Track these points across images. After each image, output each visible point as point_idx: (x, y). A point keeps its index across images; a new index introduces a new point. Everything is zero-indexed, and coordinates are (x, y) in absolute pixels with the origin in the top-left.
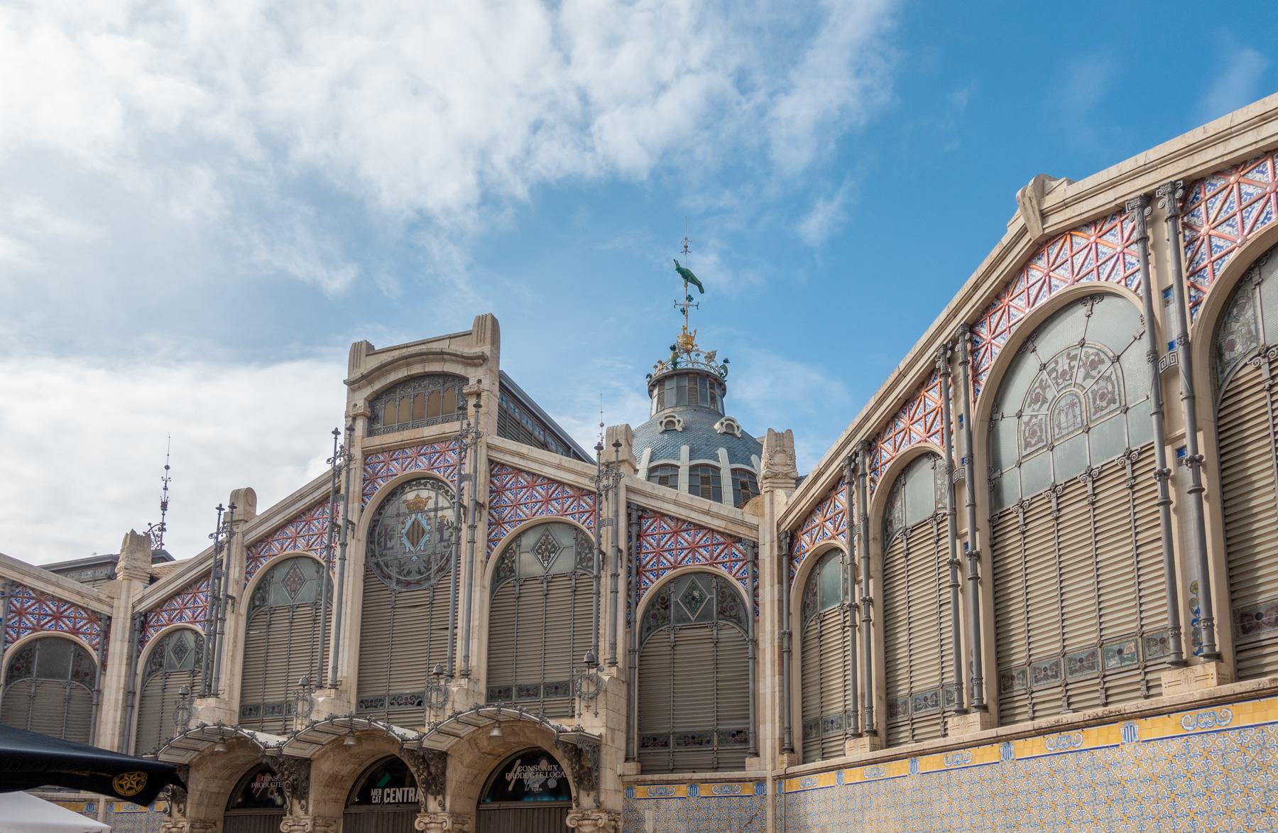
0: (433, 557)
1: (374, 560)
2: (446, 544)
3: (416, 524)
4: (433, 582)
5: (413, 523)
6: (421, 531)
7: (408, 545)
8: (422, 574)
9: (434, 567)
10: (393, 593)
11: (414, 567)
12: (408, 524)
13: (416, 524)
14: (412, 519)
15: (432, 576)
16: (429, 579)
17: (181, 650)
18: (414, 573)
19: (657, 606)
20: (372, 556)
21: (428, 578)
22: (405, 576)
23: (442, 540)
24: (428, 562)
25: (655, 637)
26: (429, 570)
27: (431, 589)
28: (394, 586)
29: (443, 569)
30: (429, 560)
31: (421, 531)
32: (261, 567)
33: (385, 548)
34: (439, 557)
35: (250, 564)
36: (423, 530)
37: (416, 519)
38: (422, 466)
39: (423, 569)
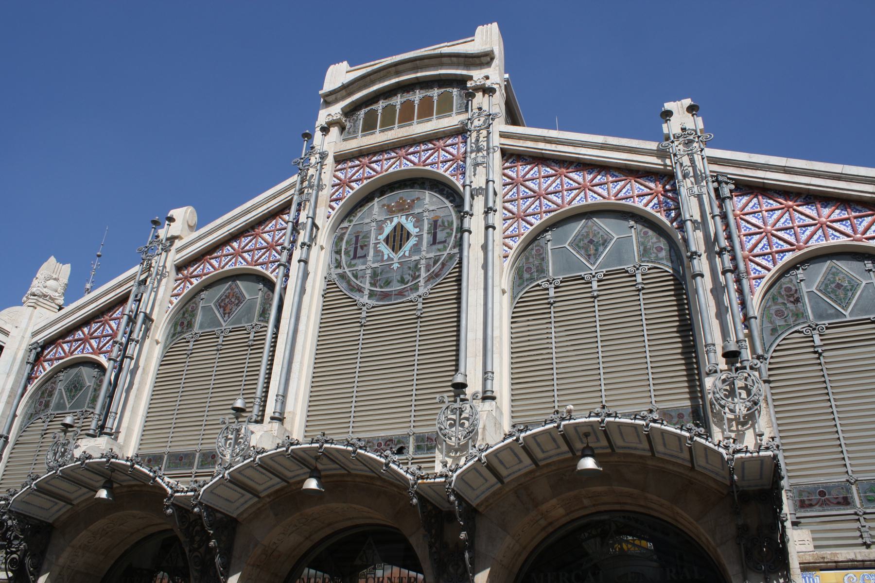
0: (423, 262)
1: (340, 271)
2: (441, 246)
3: (400, 228)
5: (395, 228)
6: (405, 236)
7: (386, 250)
8: (407, 283)
9: (423, 274)
10: (364, 308)
11: (396, 277)
12: (388, 229)
13: (400, 228)
14: (394, 224)
15: (422, 283)
17: (75, 387)
18: (395, 282)
19: (780, 300)
21: (416, 288)
22: (381, 287)
24: (416, 267)
25: (784, 342)
26: (415, 277)
27: (421, 300)
28: (365, 299)
29: (437, 275)
30: (417, 265)
31: (405, 236)
32: (191, 287)
33: (355, 257)
37: (399, 223)
39: (407, 277)
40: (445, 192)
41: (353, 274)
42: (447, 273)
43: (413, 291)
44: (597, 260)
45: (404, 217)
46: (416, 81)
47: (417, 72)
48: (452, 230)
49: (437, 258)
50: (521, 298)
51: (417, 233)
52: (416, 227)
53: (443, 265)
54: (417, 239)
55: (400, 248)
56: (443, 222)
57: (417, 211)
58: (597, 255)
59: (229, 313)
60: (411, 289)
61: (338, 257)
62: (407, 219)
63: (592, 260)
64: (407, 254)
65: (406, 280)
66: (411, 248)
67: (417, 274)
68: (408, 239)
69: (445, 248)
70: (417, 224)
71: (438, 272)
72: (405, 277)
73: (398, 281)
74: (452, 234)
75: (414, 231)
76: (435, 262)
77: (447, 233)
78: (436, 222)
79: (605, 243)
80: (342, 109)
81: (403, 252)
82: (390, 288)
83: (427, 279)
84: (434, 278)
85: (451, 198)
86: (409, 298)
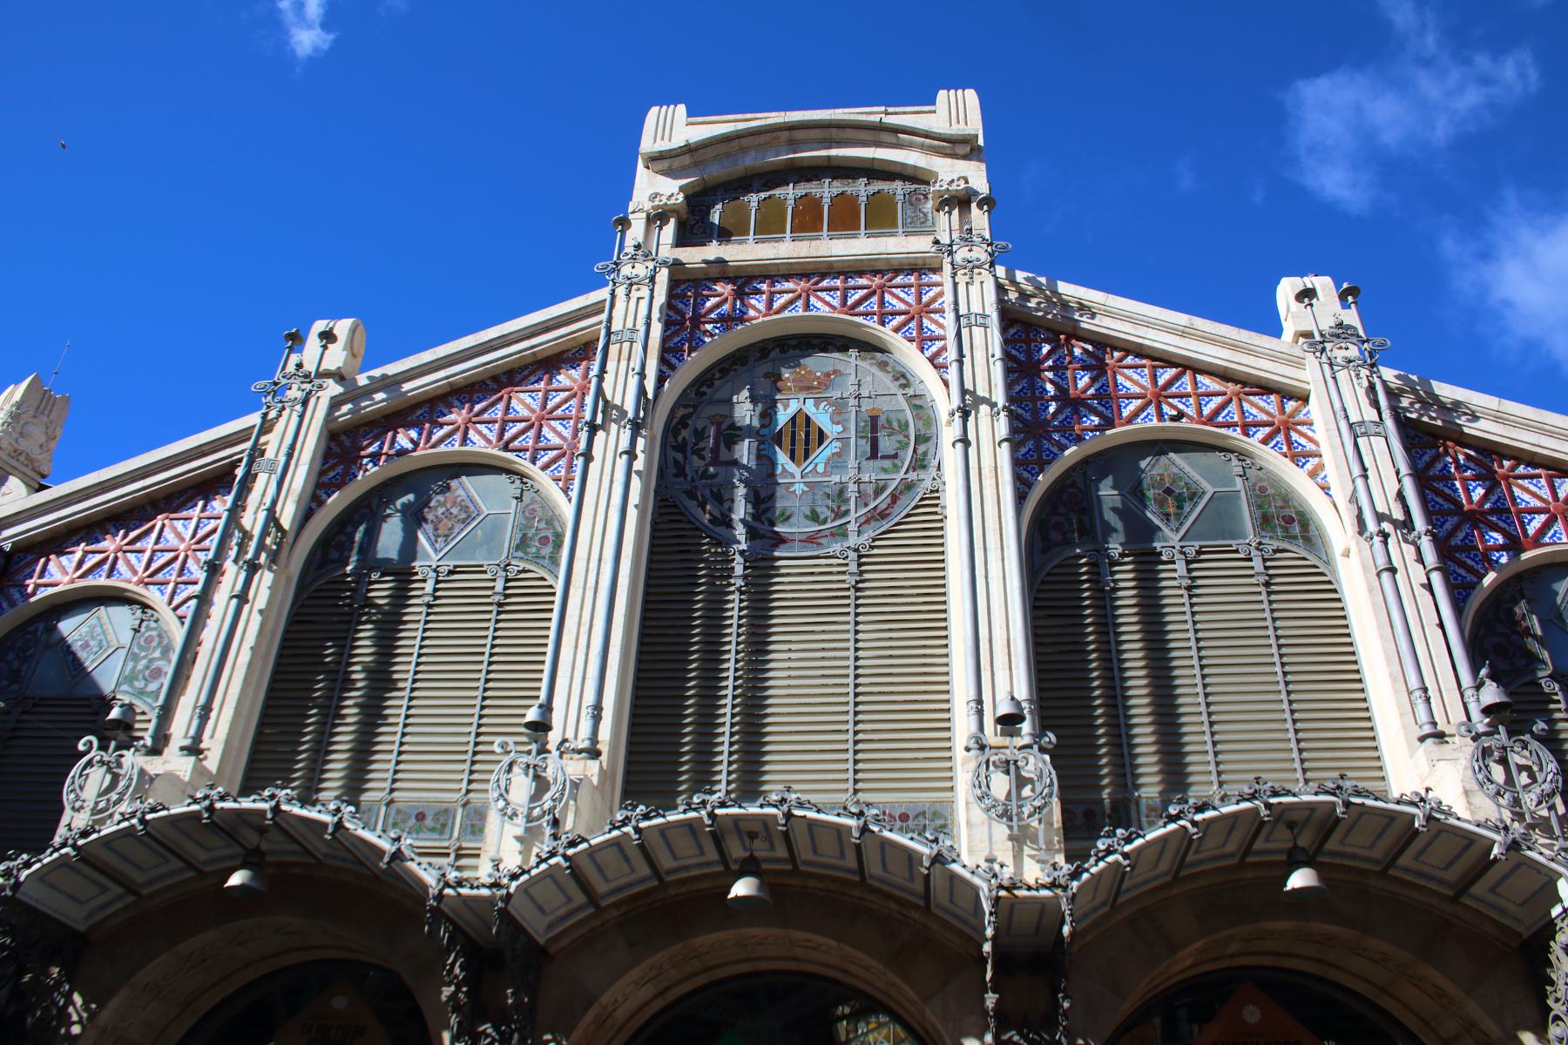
0: (852, 487)
2: (887, 464)
4: (853, 540)
5: (793, 419)
6: (814, 436)
8: (825, 522)
15: (852, 527)
16: (845, 535)
20: (676, 476)
23: (874, 454)
27: (853, 555)
29: (883, 515)
30: (841, 492)
31: (814, 436)
34: (870, 490)
35: (332, 468)
36: (821, 432)
38: (824, 307)
39: (824, 512)
40: (889, 369)
41: (711, 492)
42: (903, 514)
43: (839, 538)
44: (1182, 524)
45: (810, 403)
46: (825, 164)
47: (830, 148)
48: (907, 437)
49: (881, 483)
50: (1048, 574)
51: (839, 433)
52: (838, 423)
53: (894, 498)
54: (838, 444)
55: (806, 457)
56: (889, 421)
57: (836, 394)
58: (1180, 517)
59: (447, 536)
60: (833, 535)
61: (680, 456)
62: (817, 406)
63: (1174, 524)
64: (820, 469)
65: (822, 517)
66: (829, 459)
67: (843, 508)
68: (821, 442)
69: (897, 468)
70: (837, 418)
71: (886, 509)
72: (818, 510)
73: (806, 517)
74: (907, 445)
75: (832, 430)
76: (878, 491)
77: (899, 442)
78: (874, 420)
79: (1194, 496)
80: (680, 187)
81: (812, 466)
82: (790, 526)
83: (863, 519)
84: (877, 520)
85: (903, 381)
86: (830, 550)
